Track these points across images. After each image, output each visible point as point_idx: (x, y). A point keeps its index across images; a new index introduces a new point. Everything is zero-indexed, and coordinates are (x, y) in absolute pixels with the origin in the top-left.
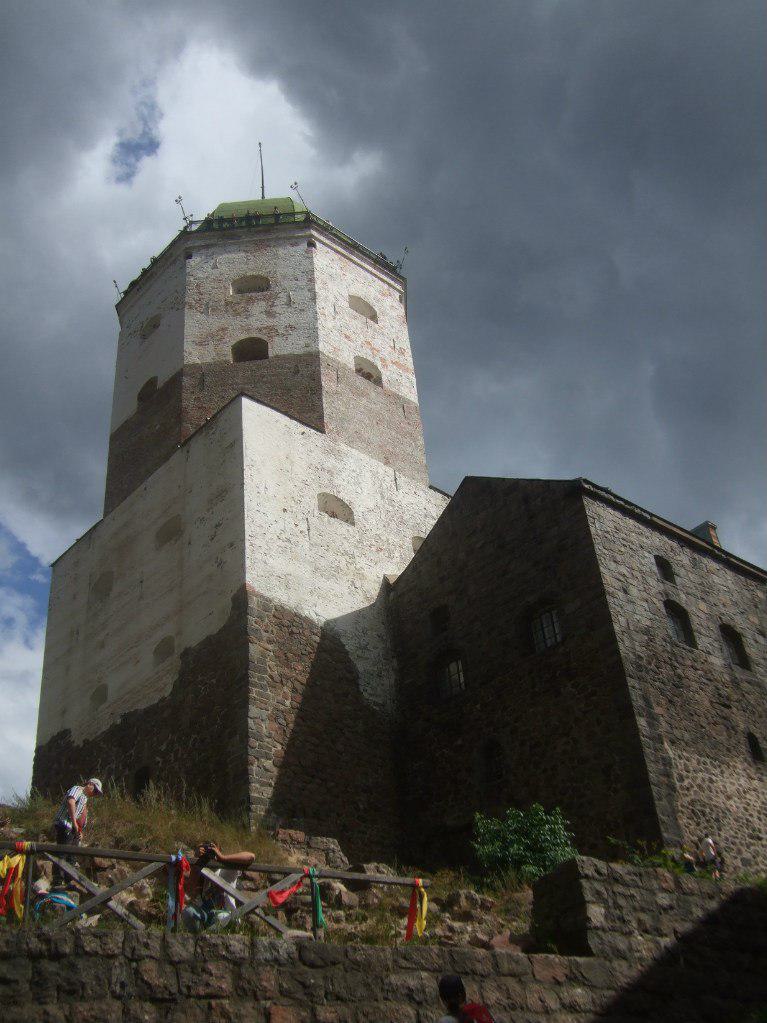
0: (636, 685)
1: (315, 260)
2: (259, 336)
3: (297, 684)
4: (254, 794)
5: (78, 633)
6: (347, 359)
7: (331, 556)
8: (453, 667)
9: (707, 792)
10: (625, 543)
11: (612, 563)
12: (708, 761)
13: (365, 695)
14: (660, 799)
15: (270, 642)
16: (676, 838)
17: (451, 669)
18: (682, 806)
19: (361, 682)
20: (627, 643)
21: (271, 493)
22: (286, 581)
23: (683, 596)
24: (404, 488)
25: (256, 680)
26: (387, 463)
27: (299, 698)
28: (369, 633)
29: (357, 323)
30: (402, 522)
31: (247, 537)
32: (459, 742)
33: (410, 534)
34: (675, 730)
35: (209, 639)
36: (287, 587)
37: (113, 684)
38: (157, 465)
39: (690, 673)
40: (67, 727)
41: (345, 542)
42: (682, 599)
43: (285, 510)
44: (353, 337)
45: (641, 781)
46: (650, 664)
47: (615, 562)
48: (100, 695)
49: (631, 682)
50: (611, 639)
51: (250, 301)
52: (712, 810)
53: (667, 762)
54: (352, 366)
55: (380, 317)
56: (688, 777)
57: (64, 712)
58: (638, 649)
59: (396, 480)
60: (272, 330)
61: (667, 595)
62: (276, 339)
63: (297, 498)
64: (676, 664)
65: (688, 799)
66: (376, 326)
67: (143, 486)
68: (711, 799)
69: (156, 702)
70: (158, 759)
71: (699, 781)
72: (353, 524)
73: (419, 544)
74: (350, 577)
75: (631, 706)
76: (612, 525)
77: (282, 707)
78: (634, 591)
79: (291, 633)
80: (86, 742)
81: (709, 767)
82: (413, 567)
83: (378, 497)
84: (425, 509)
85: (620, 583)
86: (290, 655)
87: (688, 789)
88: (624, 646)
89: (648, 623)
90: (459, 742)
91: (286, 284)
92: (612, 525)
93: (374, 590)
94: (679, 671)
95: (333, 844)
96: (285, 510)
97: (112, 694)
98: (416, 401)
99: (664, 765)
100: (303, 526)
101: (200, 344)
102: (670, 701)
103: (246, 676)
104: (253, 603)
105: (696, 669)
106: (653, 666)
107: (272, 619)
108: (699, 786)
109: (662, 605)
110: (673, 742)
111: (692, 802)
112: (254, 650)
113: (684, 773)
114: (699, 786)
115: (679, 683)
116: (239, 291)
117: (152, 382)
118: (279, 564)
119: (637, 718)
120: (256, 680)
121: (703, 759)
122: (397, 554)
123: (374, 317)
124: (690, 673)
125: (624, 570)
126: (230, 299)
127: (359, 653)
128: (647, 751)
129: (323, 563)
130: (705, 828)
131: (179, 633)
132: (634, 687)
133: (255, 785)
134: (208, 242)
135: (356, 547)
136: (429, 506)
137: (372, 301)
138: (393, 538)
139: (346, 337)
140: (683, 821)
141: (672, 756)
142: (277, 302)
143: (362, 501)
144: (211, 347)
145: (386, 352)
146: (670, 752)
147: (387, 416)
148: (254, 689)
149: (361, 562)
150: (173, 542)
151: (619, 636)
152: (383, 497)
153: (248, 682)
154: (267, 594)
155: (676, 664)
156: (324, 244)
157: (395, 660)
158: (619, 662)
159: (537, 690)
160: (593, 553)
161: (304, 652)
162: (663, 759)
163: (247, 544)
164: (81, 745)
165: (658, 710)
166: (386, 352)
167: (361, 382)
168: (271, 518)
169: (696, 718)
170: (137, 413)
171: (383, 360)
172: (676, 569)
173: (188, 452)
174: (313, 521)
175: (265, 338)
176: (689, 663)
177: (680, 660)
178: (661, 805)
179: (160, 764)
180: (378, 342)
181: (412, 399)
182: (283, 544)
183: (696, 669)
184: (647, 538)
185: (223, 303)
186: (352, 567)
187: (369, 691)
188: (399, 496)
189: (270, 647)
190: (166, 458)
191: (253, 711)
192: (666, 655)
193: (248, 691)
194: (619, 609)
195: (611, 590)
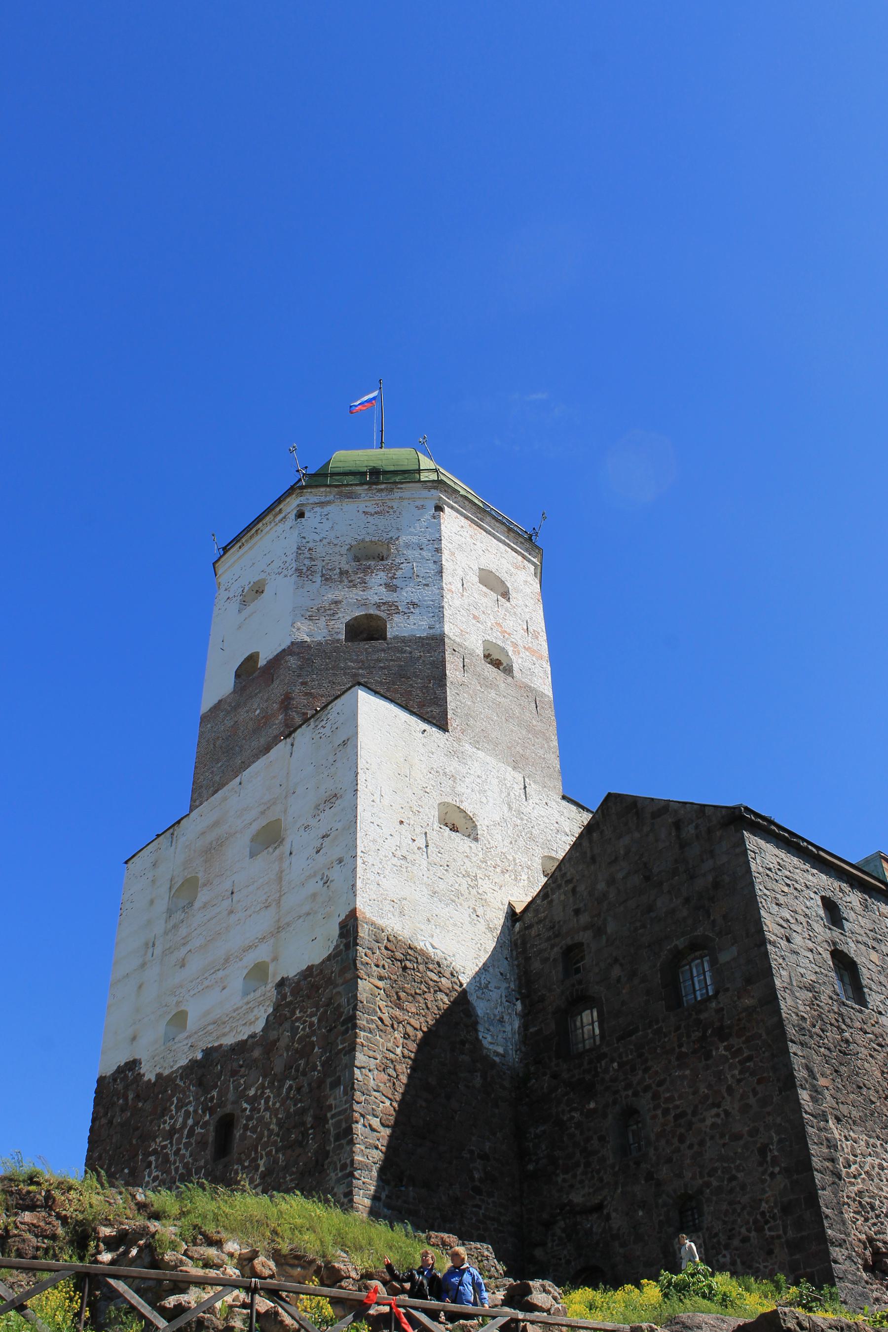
0: (800, 1053)
1: (443, 527)
2: (378, 613)
3: (409, 1029)
4: (358, 1158)
5: (154, 945)
6: (476, 645)
8: (586, 1016)
9: (876, 1180)
10: (788, 882)
11: (774, 906)
12: (878, 1143)
13: (485, 1043)
14: (824, 1189)
15: (381, 978)
16: (843, 1236)
17: (585, 1021)
18: (848, 1197)
19: (481, 1028)
20: (790, 1002)
21: (386, 801)
22: (399, 907)
23: (852, 945)
24: (534, 798)
25: (365, 1023)
26: (514, 768)
27: (413, 1047)
28: (491, 970)
29: (487, 599)
30: (532, 838)
31: (359, 853)
32: (592, 1105)
33: (539, 853)
34: (840, 1105)
35: (310, 968)
36: (402, 913)
37: (197, 1011)
38: (256, 757)
39: (859, 1037)
40: (137, 1057)
41: (466, 860)
42: (851, 949)
44: (482, 617)
45: (805, 1165)
46: (814, 1026)
47: (777, 904)
48: (180, 1019)
49: (793, 1048)
50: (771, 998)
51: (367, 570)
52: (881, 1202)
53: (832, 1145)
54: (480, 652)
55: (513, 594)
56: (855, 1163)
57: (134, 1039)
58: (801, 1008)
59: (525, 787)
60: (392, 608)
61: (835, 943)
62: (397, 618)
63: (415, 809)
64: (844, 1027)
65: (856, 1189)
66: (508, 604)
67: (238, 780)
68: (882, 1190)
69: (245, 1037)
70: (245, 1105)
71: (867, 1168)
72: (476, 839)
73: (552, 867)
74: (472, 903)
75: (793, 1077)
76: (775, 860)
77: (392, 1056)
78: (797, 939)
79: (405, 968)
80: (159, 1076)
82: (545, 893)
83: (505, 808)
84: (560, 826)
85: (782, 930)
86: (402, 995)
87: (855, 1177)
88: (786, 1004)
89: (814, 978)
90: (592, 1105)
91: (409, 553)
92: (775, 860)
93: (499, 919)
94: (847, 1035)
95: (487, 1250)
96: (401, 822)
97: (192, 1023)
98: (550, 694)
99: (829, 1147)
100: (421, 842)
101: (310, 618)
102: (836, 1071)
103: (353, 1018)
104: (364, 932)
105: (866, 1033)
106: (817, 1030)
107: (385, 952)
108: (867, 1173)
109: (829, 956)
110: (838, 1120)
111: (860, 1193)
112: (364, 987)
113: (851, 1158)
114: (867, 1173)
115: (845, 1049)
116: (357, 559)
117: (252, 658)
118: (392, 885)
119: (800, 1091)
120: (365, 1023)
121: (872, 1141)
122: (524, 877)
123: (506, 595)
124: (859, 1037)
125: (786, 914)
126: (346, 567)
128: (810, 1130)
129: (442, 886)
130: (874, 1224)
131: (275, 959)
132: (795, 1054)
133: (358, 1147)
134: (323, 499)
135: (480, 868)
136: (561, 819)
137: (504, 576)
138: (522, 859)
139: (475, 617)
140: (848, 1215)
141: (837, 1136)
142: (399, 573)
143: (487, 813)
144: (322, 622)
145: (519, 636)
146: (835, 1132)
147: (517, 712)
148: (362, 1033)
149: (485, 885)
150: (270, 849)
151: (780, 994)
152: (510, 808)
153: (355, 1026)
154: (380, 922)
155: (844, 1027)
156: (452, 508)
157: (519, 1003)
158: (780, 1024)
159: (684, 1049)
160: (754, 896)
161: (418, 991)
162: (827, 1140)
163: (359, 861)
164: (153, 1080)
165: (822, 1082)
166: (519, 636)
167: (490, 671)
169: (864, 1091)
170: (234, 692)
171: (515, 645)
172: (846, 913)
173: (292, 745)
174: (433, 836)
175: (383, 615)
176: (858, 1025)
177: (848, 1021)
178: (825, 1195)
179: (248, 1112)
180: (510, 624)
181: (546, 692)
182: (399, 863)
183: (866, 1033)
184: (813, 875)
185: (338, 571)
186: (474, 891)
187: (489, 1039)
188: (527, 807)
189: (381, 984)
190: (267, 749)
191: (360, 1058)
192: (831, 1015)
193: (356, 1036)
194: (781, 961)
195: (772, 938)
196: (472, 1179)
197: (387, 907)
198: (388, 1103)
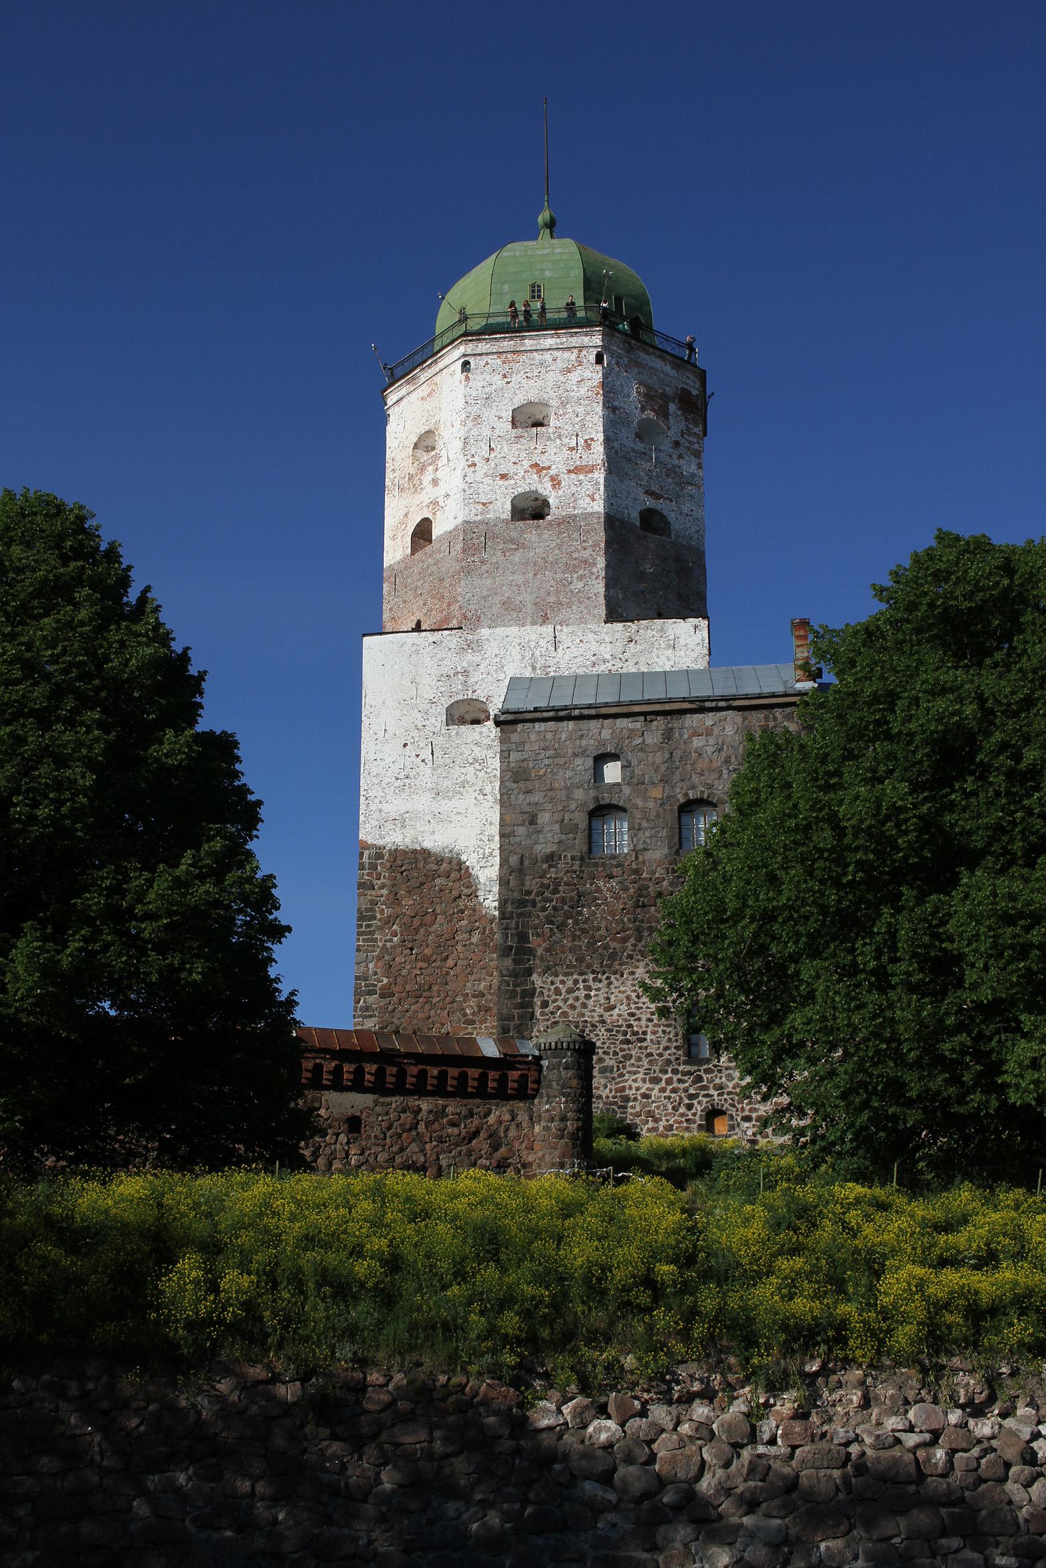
7: (457, 772)
15: (383, 887)
19: (480, 893)
22: (401, 821)
43: (405, 745)
77: (388, 945)
81: (591, 983)
96: (405, 745)
118: (396, 805)
127: (482, 864)
154: (380, 843)
168: (388, 760)
174: (439, 741)
196: (465, 1015)
197: (389, 826)
198: (385, 980)
